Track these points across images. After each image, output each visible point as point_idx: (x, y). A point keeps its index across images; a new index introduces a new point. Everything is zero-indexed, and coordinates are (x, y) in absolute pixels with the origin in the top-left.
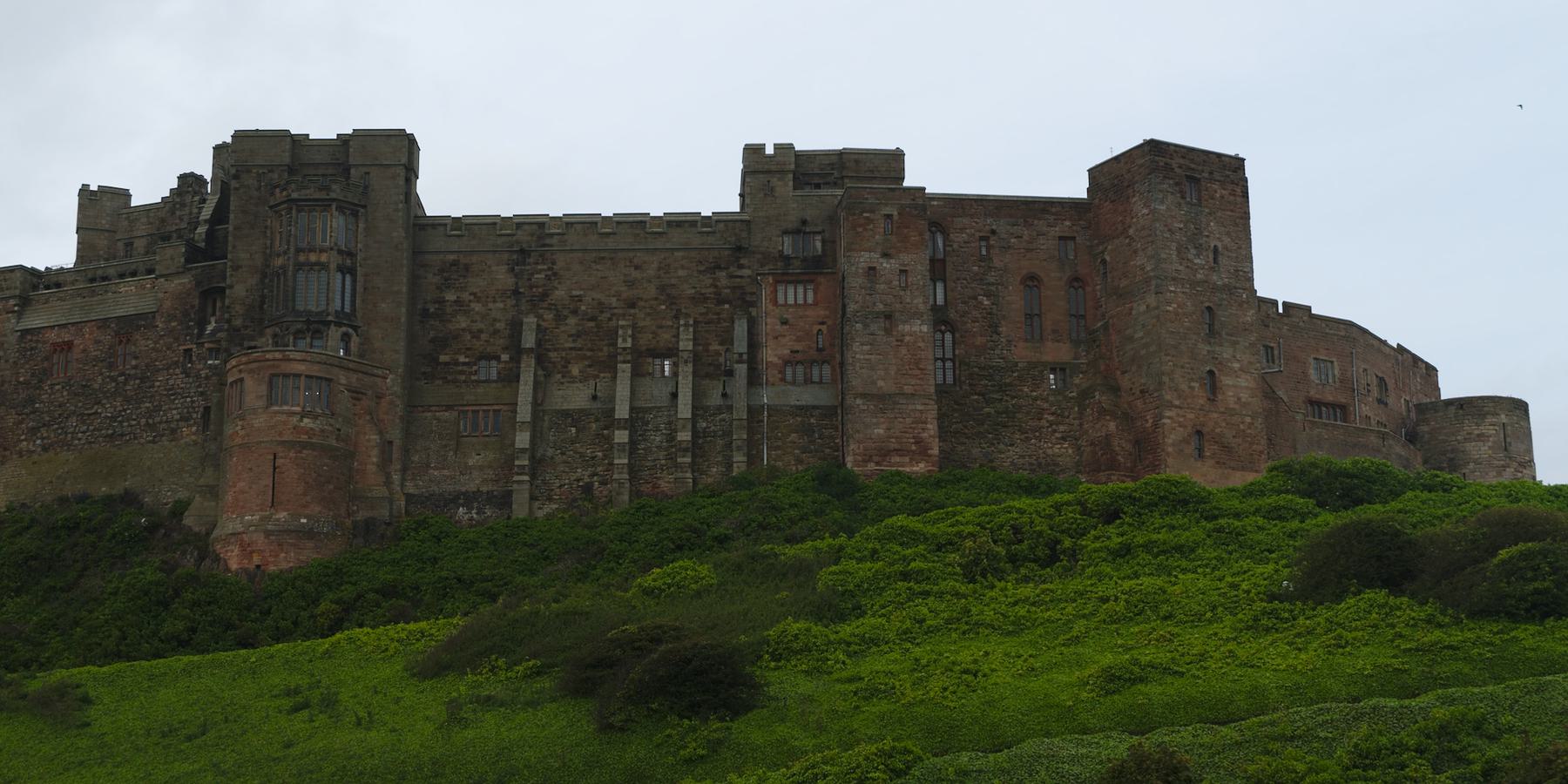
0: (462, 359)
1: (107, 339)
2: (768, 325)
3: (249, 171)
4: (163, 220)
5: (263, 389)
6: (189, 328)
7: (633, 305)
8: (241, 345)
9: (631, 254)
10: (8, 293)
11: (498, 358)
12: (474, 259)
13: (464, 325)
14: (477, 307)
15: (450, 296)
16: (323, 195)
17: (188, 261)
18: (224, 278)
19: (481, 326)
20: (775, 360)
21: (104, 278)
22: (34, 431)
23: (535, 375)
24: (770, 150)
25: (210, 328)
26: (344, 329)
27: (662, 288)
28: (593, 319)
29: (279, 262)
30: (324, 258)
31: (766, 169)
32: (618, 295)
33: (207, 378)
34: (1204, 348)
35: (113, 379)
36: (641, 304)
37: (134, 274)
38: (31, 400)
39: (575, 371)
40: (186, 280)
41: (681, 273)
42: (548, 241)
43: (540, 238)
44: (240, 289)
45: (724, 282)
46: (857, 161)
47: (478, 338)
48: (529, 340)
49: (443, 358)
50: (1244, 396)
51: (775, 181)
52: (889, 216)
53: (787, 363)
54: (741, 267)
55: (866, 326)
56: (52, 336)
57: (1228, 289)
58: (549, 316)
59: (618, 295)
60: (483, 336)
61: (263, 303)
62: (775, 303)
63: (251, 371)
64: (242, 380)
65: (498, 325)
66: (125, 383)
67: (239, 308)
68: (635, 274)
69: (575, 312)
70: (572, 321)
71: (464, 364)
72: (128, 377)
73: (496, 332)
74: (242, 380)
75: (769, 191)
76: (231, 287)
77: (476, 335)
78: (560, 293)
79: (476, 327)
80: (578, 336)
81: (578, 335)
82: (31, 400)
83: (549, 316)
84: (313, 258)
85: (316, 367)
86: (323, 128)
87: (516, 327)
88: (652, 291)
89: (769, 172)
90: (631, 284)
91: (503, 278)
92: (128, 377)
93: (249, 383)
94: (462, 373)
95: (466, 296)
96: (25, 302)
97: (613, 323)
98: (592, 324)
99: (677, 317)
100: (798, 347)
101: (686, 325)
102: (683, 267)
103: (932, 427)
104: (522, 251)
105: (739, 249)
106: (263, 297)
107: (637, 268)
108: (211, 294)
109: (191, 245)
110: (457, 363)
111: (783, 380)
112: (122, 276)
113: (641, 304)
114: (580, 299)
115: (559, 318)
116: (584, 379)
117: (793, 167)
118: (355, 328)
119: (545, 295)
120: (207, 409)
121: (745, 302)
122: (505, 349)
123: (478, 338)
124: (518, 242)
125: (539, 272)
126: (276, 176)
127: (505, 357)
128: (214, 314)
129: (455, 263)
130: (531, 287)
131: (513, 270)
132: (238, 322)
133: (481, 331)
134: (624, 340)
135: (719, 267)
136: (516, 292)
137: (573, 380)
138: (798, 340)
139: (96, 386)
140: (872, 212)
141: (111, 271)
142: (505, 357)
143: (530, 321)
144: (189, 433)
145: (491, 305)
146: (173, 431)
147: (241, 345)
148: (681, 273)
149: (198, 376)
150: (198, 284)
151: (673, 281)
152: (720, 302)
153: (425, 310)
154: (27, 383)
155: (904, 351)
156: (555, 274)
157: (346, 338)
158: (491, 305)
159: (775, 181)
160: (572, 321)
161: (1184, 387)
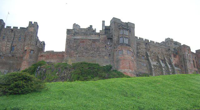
1: (91, 42)
11: (144, 56)
15: (138, 47)
16: (127, 28)
22: (77, 54)
27: (162, 52)
29: (120, 36)
30: (127, 37)
37: (92, 34)
38: (76, 49)
39: (153, 60)
44: (115, 38)
45: (168, 53)
65: (144, 52)
69: (153, 53)
72: (95, 48)
73: (144, 53)
77: (142, 53)
78: (151, 50)
81: (153, 56)
82: (76, 49)
84: (126, 36)
86: (124, 20)
87: (146, 53)
91: (145, 47)
92: (95, 48)
93: (124, 50)
96: (74, 35)
105: (169, 49)
119: (149, 50)
120: (110, 55)
122: (145, 55)
127: (145, 56)
129: (139, 43)
142: (145, 56)
143: (148, 52)
144: (106, 58)
150: (107, 37)
154: (75, 46)
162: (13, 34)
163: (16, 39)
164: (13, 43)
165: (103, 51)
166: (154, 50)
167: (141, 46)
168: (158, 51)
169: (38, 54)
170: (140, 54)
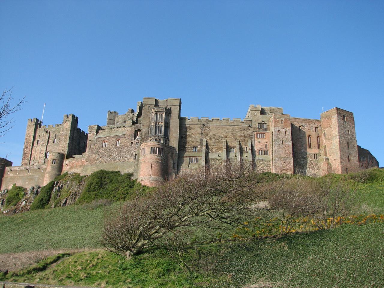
0: (190, 147)
2: (256, 142)
3: (146, 106)
4: (125, 118)
5: (150, 150)
6: (132, 138)
7: (226, 137)
8: (144, 141)
9: (226, 126)
10: (94, 130)
12: (193, 126)
13: (190, 140)
14: (193, 136)
17: (132, 124)
18: (140, 128)
19: (194, 140)
21: (114, 128)
23: (206, 151)
25: (136, 138)
26: (166, 139)
27: (233, 134)
28: (217, 140)
32: (223, 135)
33: (136, 148)
34: (347, 151)
35: (116, 148)
36: (228, 137)
37: (120, 127)
39: (214, 150)
40: (132, 128)
41: (237, 131)
42: (208, 123)
43: (207, 122)
44: (144, 130)
46: (273, 110)
47: (193, 142)
48: (204, 143)
50: (355, 161)
54: (249, 130)
55: (278, 143)
56: (102, 139)
57: (351, 139)
58: (208, 138)
59: (223, 135)
60: (194, 142)
61: (148, 133)
63: (147, 146)
64: (145, 148)
65: (198, 140)
66: (118, 149)
67: (143, 134)
69: (214, 138)
73: (197, 141)
74: (145, 148)
76: (142, 129)
77: (193, 142)
78: (211, 134)
79: (193, 140)
80: (215, 143)
83: (208, 138)
87: (201, 140)
88: (230, 134)
90: (226, 133)
93: (146, 149)
94: (190, 150)
95: (191, 134)
96: (97, 133)
97: (222, 141)
98: (218, 141)
99: (235, 140)
101: (238, 142)
102: (237, 130)
104: (203, 125)
106: (149, 132)
107: (227, 129)
108: (137, 131)
109: (133, 121)
110: (189, 148)
112: (117, 127)
113: (228, 137)
115: (210, 139)
116: (216, 152)
117: (260, 110)
119: (207, 134)
120: (136, 155)
121: (251, 137)
123: (193, 142)
124: (202, 123)
125: (206, 129)
126: (152, 107)
127: (199, 147)
128: (137, 135)
130: (205, 132)
131: (201, 128)
132: (143, 137)
133: (194, 141)
134: (225, 144)
135: (245, 130)
136: (202, 133)
137: (213, 152)
138: (261, 146)
139: (112, 150)
140: (279, 119)
141: (115, 127)
142: (199, 147)
143: (204, 139)
144: (132, 160)
145: (196, 136)
146: (128, 159)
147: (144, 141)
148: (237, 131)
149: (134, 148)
150: (134, 129)
152: (245, 137)
153: (182, 136)
156: (210, 130)
158: (196, 136)
159: (256, 112)
160: (213, 140)
161: (344, 158)
162: (47, 135)
163: (51, 141)
164: (48, 148)
165: (128, 151)
166: (218, 133)
168: (226, 133)
169: (62, 164)
170: (189, 145)
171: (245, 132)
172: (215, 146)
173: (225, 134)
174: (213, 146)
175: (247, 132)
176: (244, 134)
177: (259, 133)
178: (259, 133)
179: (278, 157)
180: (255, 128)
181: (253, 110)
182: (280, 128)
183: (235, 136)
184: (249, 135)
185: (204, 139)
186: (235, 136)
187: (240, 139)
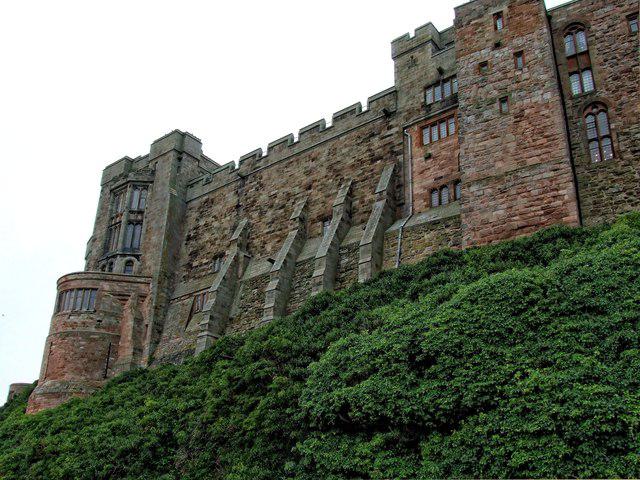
0: (205, 261)
7: (309, 188)
14: (216, 224)
20: (421, 191)
24: (412, 35)
26: (128, 258)
27: (330, 168)
31: (405, 51)
49: (195, 264)
51: (416, 54)
52: (498, 15)
53: (432, 191)
54: (390, 128)
55: (478, 116)
62: (421, 144)
68: (312, 164)
69: (271, 207)
70: (269, 213)
71: (206, 264)
75: (414, 62)
83: (255, 215)
85: (84, 282)
88: (324, 171)
89: (412, 50)
94: (204, 270)
98: (282, 211)
100: (441, 173)
102: (346, 146)
103: (567, 192)
111: (430, 206)
114: (275, 196)
118: (137, 257)
135: (373, 135)
136: (238, 206)
138: (442, 167)
151: (339, 159)
152: (373, 161)
155: (524, 124)
157: (129, 263)
167: (217, 209)
171: (376, 142)
172: (274, 231)
173: (306, 180)
174: (267, 233)
175: (382, 138)
176: (370, 150)
177: (432, 120)
178: (432, 120)
179: (479, 181)
180: (410, 112)
181: (404, 50)
182: (485, 54)
183: (337, 173)
184: (388, 148)
185: (244, 222)
186: (337, 173)
187: (354, 175)
